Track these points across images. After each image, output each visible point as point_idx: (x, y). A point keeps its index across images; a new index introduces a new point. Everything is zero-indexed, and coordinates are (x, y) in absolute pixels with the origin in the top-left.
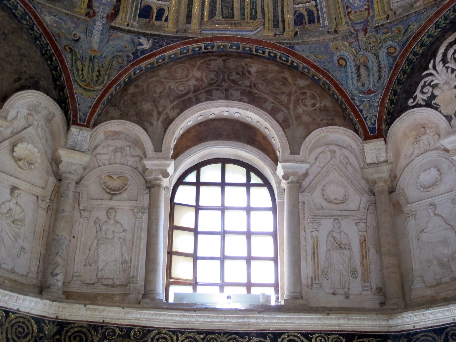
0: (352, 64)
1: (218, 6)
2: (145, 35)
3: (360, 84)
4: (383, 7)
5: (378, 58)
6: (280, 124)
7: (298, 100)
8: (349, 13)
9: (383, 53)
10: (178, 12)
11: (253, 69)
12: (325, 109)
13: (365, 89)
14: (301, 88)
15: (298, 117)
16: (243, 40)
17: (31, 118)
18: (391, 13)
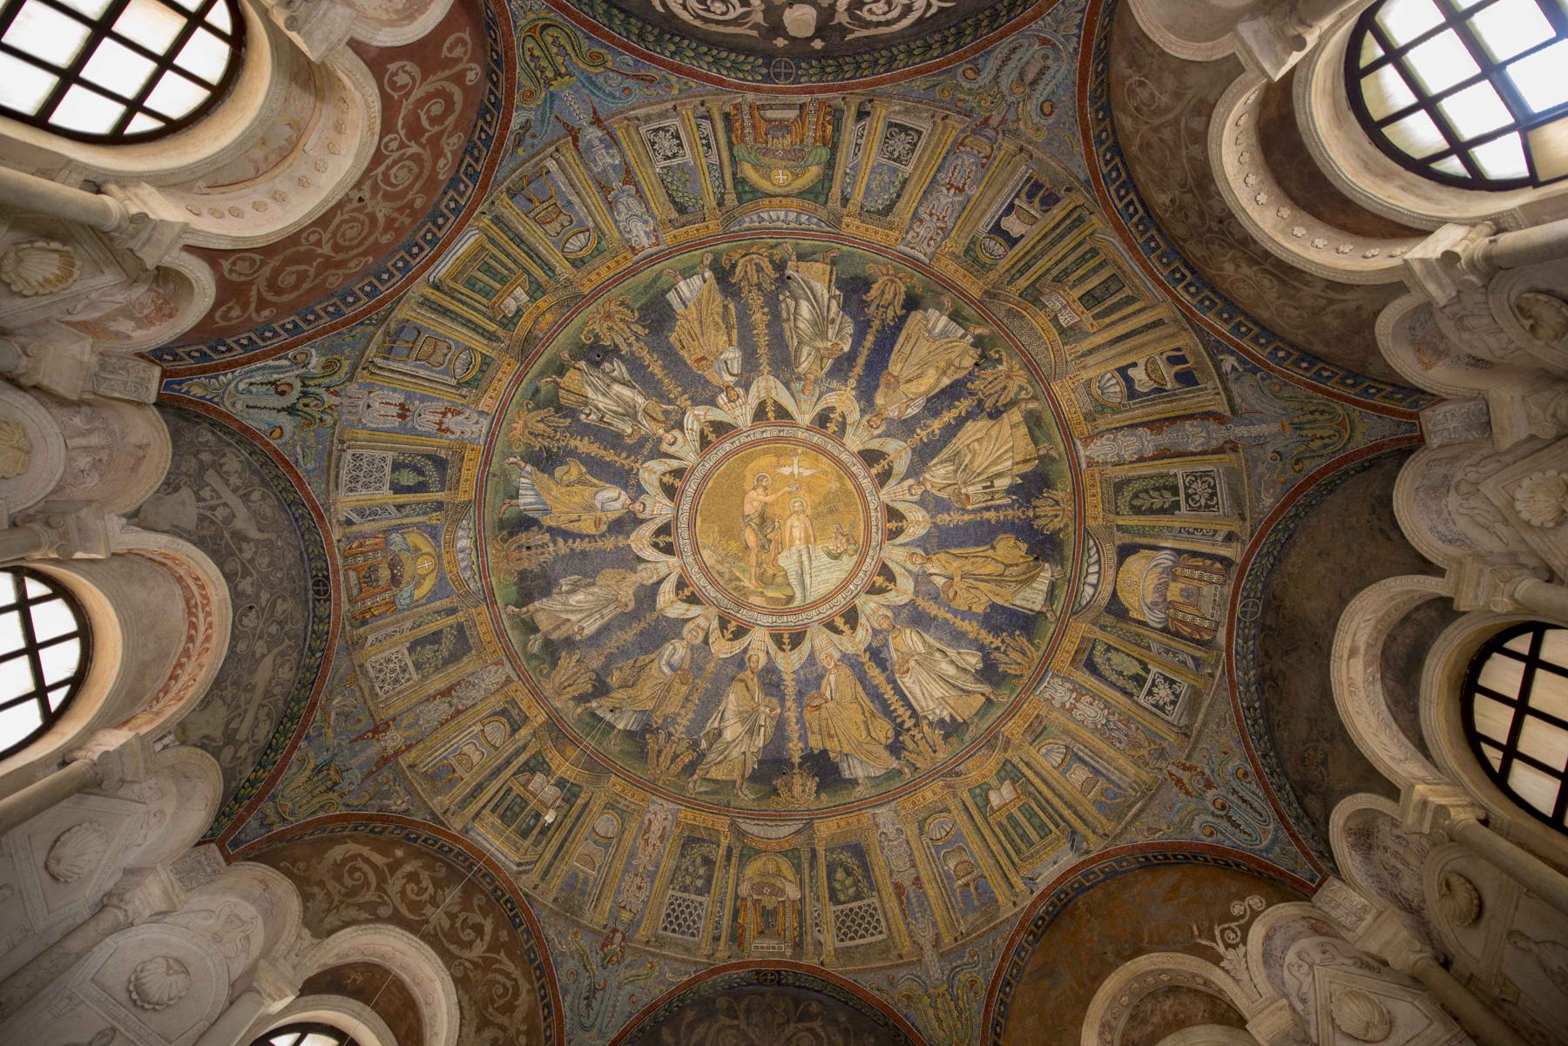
0: (1037, 94)
1: (1114, 300)
2: (1218, 366)
3: (1049, 62)
4: (943, 133)
5: (996, 77)
6: (1209, 117)
7: (1154, 113)
8: (987, 157)
9: (986, 77)
10: (1159, 340)
11: (1164, 198)
12: (1133, 63)
13: (1047, 50)
14: (1135, 119)
15: (1177, 96)
16: (1132, 248)
17: (1464, 488)
18: (939, 121)
